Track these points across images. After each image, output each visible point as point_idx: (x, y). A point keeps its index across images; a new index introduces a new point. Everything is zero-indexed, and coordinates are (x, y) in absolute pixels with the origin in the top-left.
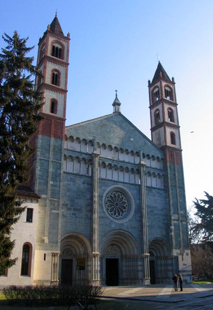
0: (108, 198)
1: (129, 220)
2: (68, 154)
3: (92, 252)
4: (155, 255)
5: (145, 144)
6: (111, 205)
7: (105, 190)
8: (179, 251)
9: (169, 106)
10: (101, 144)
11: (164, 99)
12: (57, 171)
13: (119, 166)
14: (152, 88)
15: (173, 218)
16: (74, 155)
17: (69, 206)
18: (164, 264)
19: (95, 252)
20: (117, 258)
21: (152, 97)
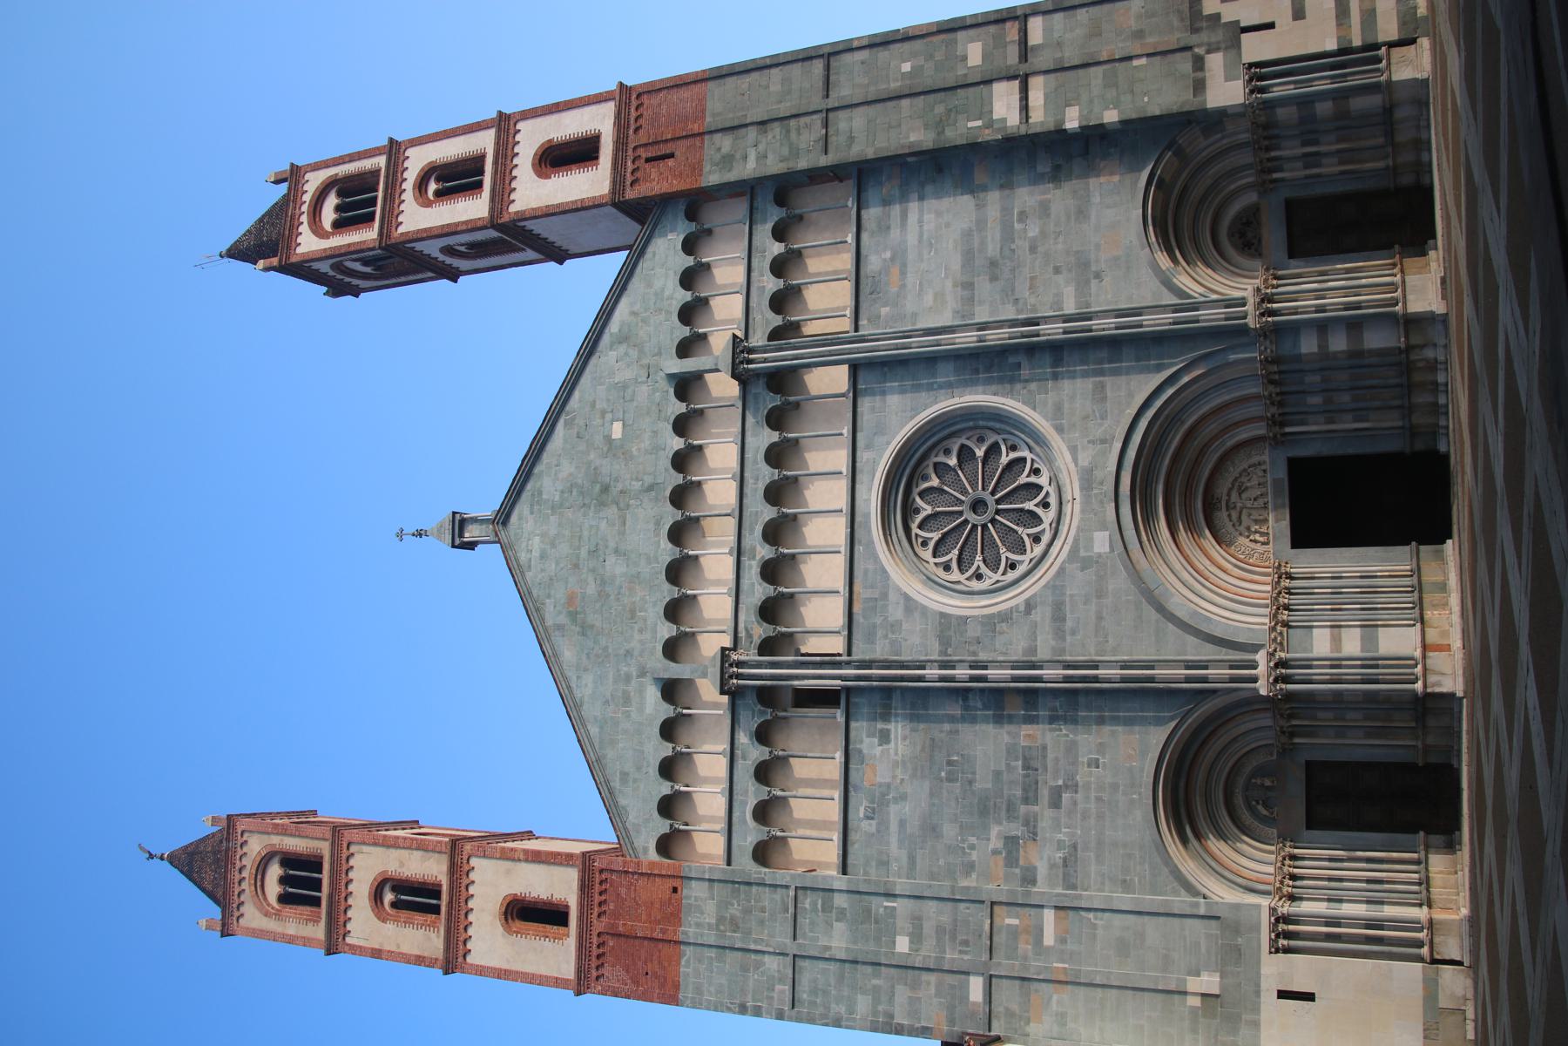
0: (947, 567)
1: (1059, 429)
2: (750, 834)
3: (1256, 690)
4: (1251, 198)
5: (623, 339)
6: (988, 543)
7: (907, 598)
8: (1215, 62)
9: (409, 195)
10: (667, 630)
11: (381, 234)
12: (842, 912)
13: (769, 513)
14: (355, 282)
15: (1014, 120)
16: (751, 794)
17: (1016, 829)
18: (1304, 144)
19: (1254, 680)
20: (1282, 473)
21: (399, 275)
